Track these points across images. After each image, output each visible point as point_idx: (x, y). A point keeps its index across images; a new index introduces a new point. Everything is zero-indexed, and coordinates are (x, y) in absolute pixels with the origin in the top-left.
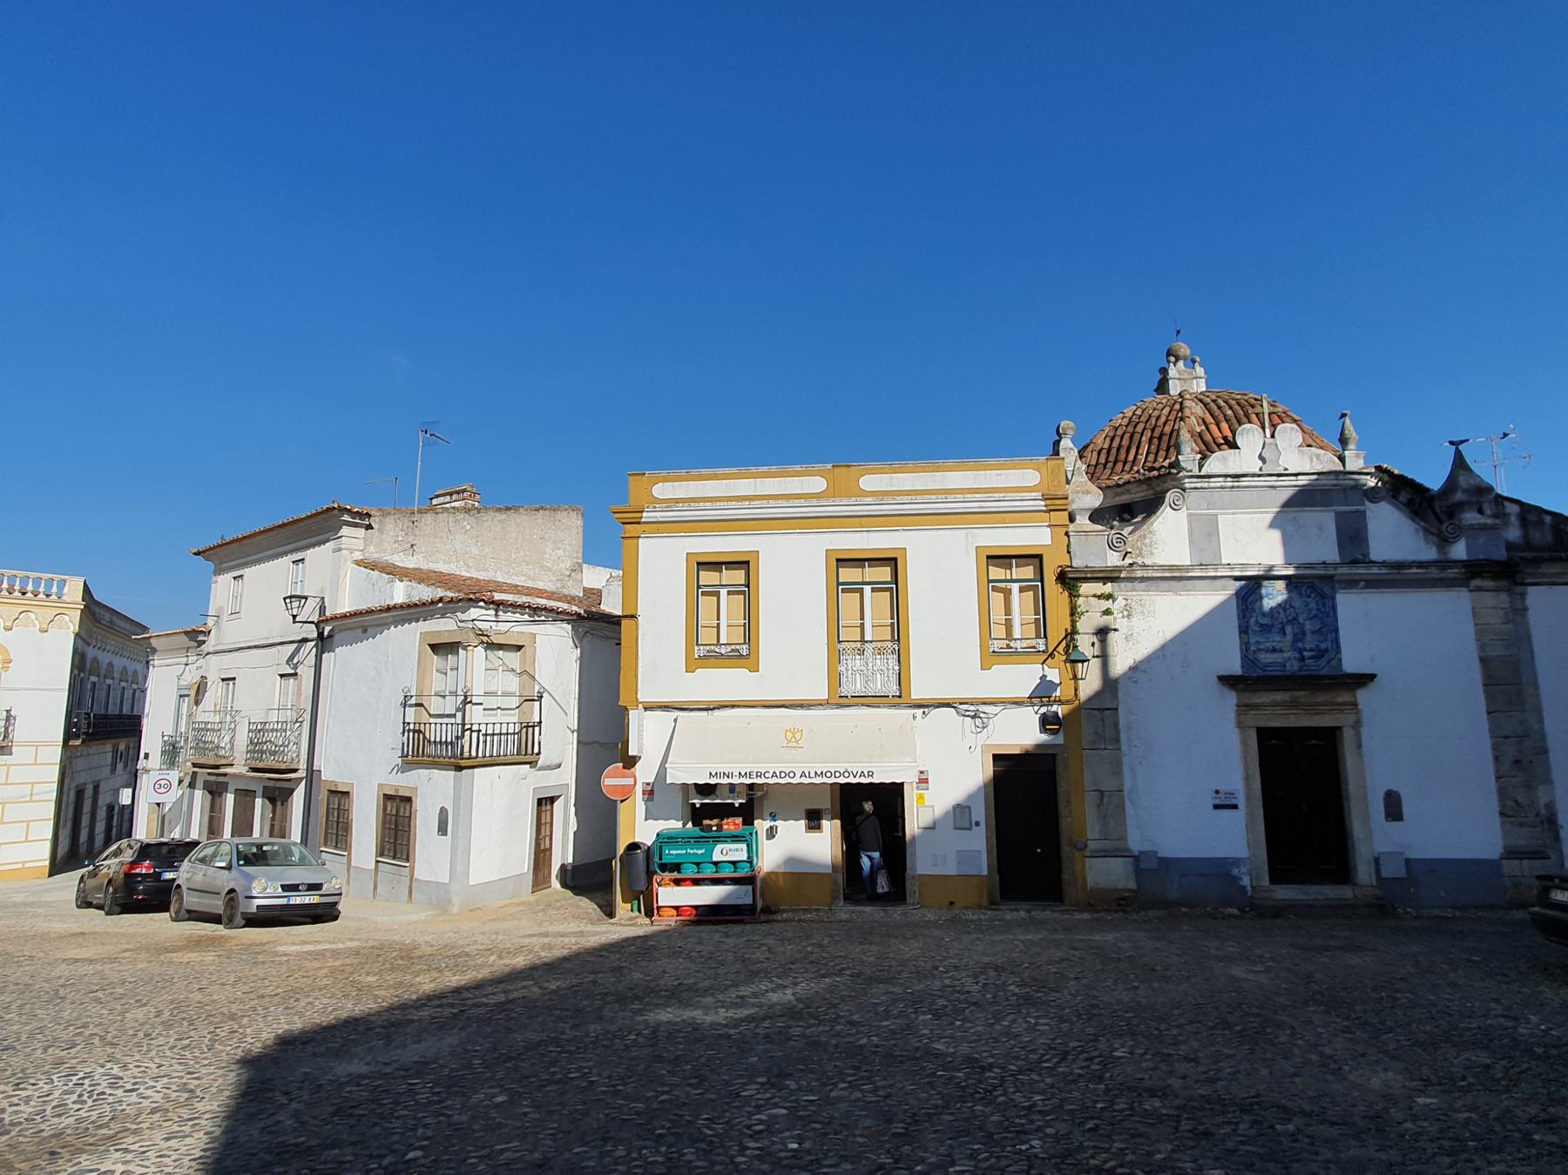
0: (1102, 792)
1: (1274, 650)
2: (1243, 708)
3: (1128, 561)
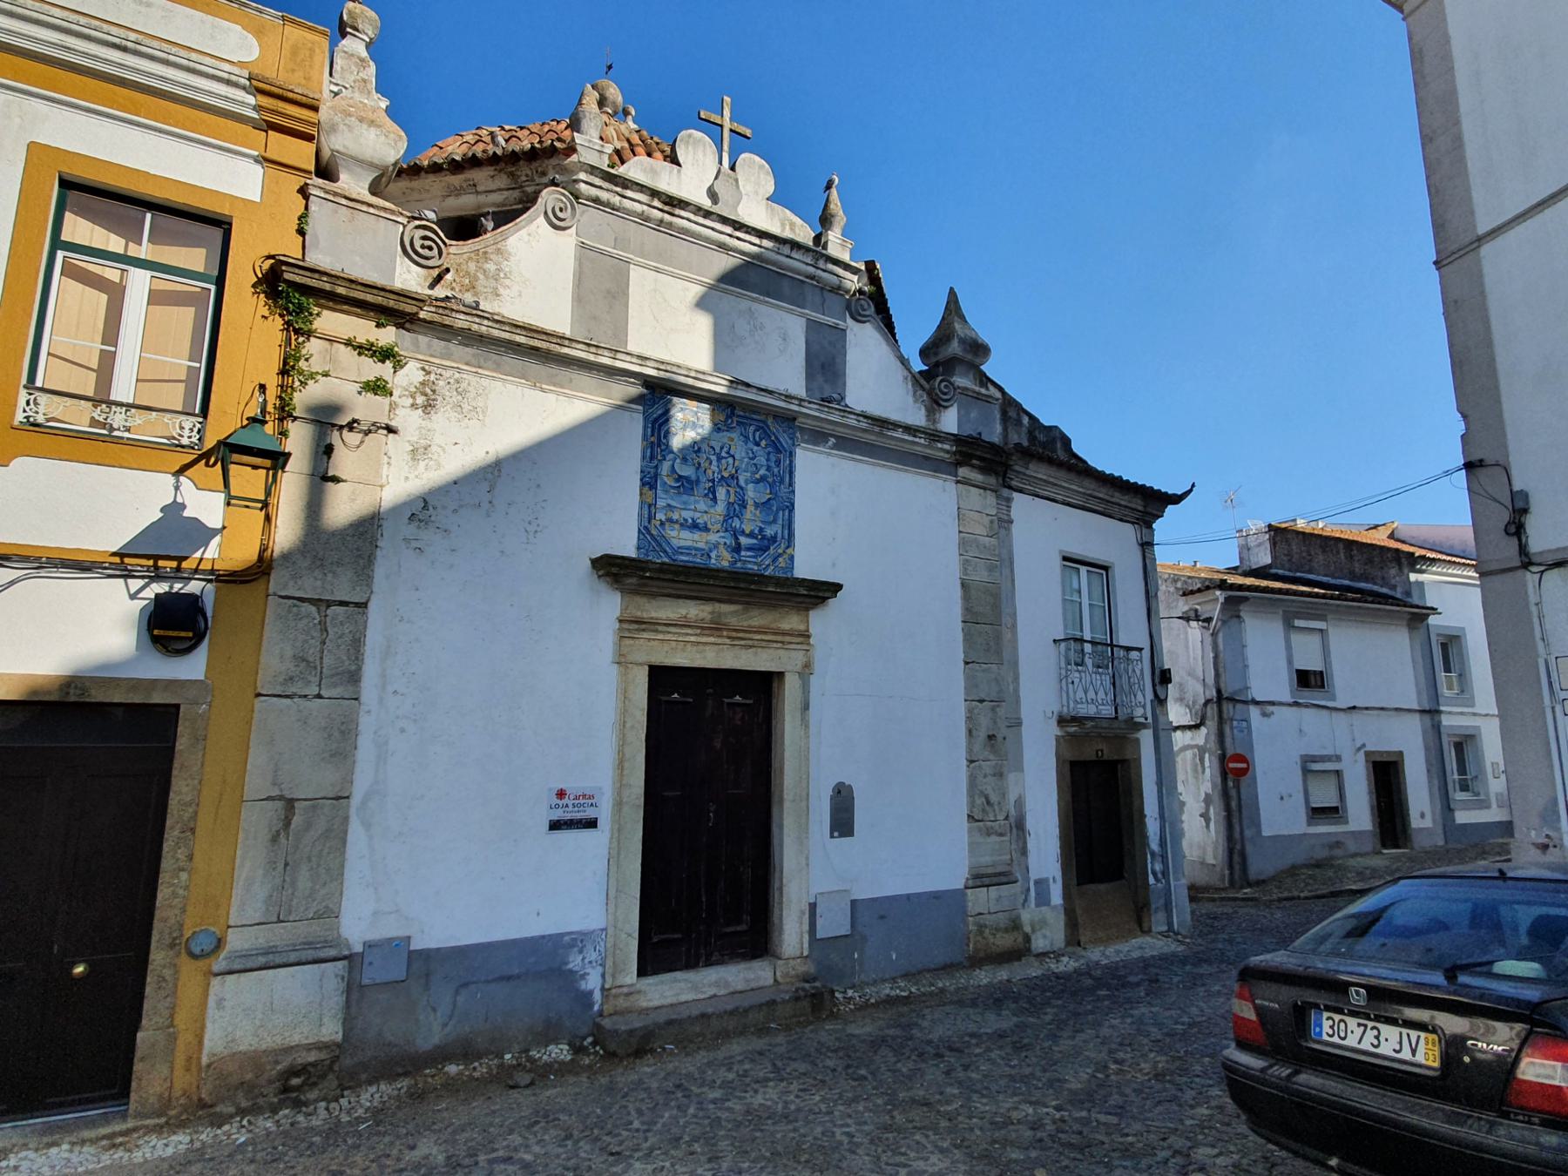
0: (290, 804)
1: (695, 526)
2: (632, 625)
3: (440, 292)
